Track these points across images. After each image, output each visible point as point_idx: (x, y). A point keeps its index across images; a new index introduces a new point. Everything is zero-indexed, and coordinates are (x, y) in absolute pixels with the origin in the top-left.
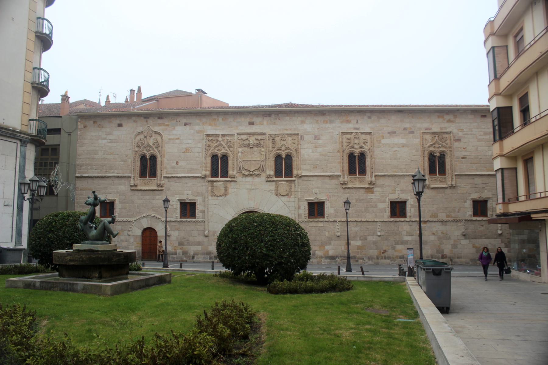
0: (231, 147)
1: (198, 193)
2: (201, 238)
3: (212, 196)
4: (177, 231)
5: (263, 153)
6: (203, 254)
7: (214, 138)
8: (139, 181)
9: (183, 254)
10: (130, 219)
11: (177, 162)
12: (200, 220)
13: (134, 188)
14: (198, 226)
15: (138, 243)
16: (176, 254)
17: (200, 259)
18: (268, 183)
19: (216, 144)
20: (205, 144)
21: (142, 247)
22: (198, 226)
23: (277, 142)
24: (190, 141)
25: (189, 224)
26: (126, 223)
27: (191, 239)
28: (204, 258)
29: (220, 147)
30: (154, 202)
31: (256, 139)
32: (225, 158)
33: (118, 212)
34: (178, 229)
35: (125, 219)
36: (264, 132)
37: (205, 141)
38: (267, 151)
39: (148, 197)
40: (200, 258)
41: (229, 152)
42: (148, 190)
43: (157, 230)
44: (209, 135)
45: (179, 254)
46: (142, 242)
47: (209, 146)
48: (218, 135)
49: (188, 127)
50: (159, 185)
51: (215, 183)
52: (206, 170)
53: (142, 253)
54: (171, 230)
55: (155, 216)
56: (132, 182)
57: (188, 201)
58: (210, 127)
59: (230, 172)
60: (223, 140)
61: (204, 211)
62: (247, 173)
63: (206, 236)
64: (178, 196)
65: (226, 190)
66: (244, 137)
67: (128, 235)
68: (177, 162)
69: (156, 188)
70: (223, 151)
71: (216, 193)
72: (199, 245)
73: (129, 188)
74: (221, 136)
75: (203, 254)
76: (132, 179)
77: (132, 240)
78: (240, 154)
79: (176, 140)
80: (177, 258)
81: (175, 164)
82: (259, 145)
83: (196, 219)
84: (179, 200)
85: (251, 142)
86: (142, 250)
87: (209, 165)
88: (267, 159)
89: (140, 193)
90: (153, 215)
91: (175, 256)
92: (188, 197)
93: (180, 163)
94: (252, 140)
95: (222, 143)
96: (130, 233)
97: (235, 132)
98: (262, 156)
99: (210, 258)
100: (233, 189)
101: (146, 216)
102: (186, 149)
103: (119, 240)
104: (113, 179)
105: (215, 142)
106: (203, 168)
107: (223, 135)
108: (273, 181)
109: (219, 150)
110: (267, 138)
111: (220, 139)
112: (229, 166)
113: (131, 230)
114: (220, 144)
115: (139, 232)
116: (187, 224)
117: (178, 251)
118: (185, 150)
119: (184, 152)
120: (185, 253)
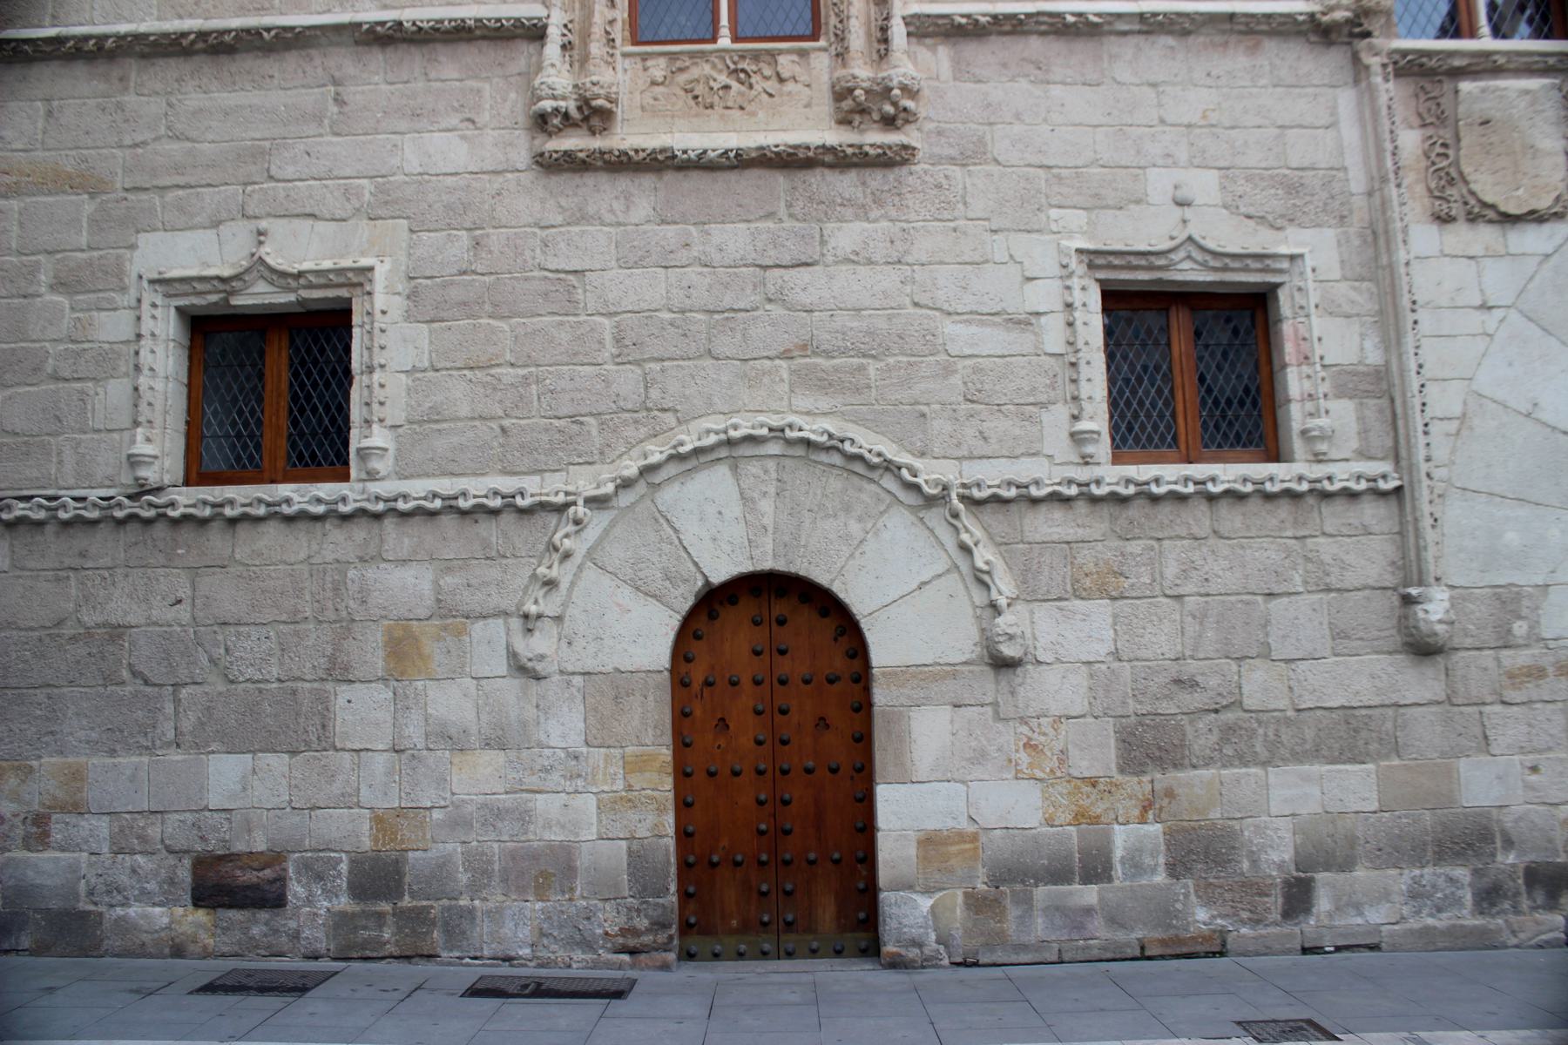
1: (1293, 188)
2: (1370, 677)
3: (1444, 219)
4: (1100, 610)
6: (1403, 850)
8: (620, 76)
9: (1174, 870)
10: (534, 488)
12: (1342, 474)
13: (575, 146)
14: (1326, 548)
15: (633, 766)
16: (1095, 868)
17: (1376, 916)
21: (683, 805)
22: (1326, 548)
25: (1232, 519)
26: (488, 530)
27: (1260, 686)
28: (1416, 894)
30: (807, 286)
33: (395, 413)
34: (1105, 585)
35: (477, 487)
39: (734, 239)
40: (1367, 901)
42: (740, 162)
43: (858, 596)
45: (1135, 865)
46: (681, 744)
50: (851, 105)
51: (1466, 86)
53: (684, 866)
54: (1030, 595)
55: (833, 446)
56: (558, 79)
57: (1189, 272)
63: (1423, 649)
64: (1076, 218)
67: (523, 670)
69: (822, 133)
72: (1356, 757)
73: (520, 147)
75: (1403, 850)
76: (552, 50)
77: (565, 726)
80: (1113, 921)
83: (1299, 467)
84: (1093, 258)
86: (684, 835)
89: (642, 197)
90: (813, 429)
91: (1090, 894)
92: (1190, 221)
96: (541, 643)
99: (1489, 896)
101: (732, 447)
103: (414, 733)
104: (343, 61)
113: (550, 606)
115: (646, 637)
116: (1198, 518)
117: (1121, 838)
120: (1200, 852)
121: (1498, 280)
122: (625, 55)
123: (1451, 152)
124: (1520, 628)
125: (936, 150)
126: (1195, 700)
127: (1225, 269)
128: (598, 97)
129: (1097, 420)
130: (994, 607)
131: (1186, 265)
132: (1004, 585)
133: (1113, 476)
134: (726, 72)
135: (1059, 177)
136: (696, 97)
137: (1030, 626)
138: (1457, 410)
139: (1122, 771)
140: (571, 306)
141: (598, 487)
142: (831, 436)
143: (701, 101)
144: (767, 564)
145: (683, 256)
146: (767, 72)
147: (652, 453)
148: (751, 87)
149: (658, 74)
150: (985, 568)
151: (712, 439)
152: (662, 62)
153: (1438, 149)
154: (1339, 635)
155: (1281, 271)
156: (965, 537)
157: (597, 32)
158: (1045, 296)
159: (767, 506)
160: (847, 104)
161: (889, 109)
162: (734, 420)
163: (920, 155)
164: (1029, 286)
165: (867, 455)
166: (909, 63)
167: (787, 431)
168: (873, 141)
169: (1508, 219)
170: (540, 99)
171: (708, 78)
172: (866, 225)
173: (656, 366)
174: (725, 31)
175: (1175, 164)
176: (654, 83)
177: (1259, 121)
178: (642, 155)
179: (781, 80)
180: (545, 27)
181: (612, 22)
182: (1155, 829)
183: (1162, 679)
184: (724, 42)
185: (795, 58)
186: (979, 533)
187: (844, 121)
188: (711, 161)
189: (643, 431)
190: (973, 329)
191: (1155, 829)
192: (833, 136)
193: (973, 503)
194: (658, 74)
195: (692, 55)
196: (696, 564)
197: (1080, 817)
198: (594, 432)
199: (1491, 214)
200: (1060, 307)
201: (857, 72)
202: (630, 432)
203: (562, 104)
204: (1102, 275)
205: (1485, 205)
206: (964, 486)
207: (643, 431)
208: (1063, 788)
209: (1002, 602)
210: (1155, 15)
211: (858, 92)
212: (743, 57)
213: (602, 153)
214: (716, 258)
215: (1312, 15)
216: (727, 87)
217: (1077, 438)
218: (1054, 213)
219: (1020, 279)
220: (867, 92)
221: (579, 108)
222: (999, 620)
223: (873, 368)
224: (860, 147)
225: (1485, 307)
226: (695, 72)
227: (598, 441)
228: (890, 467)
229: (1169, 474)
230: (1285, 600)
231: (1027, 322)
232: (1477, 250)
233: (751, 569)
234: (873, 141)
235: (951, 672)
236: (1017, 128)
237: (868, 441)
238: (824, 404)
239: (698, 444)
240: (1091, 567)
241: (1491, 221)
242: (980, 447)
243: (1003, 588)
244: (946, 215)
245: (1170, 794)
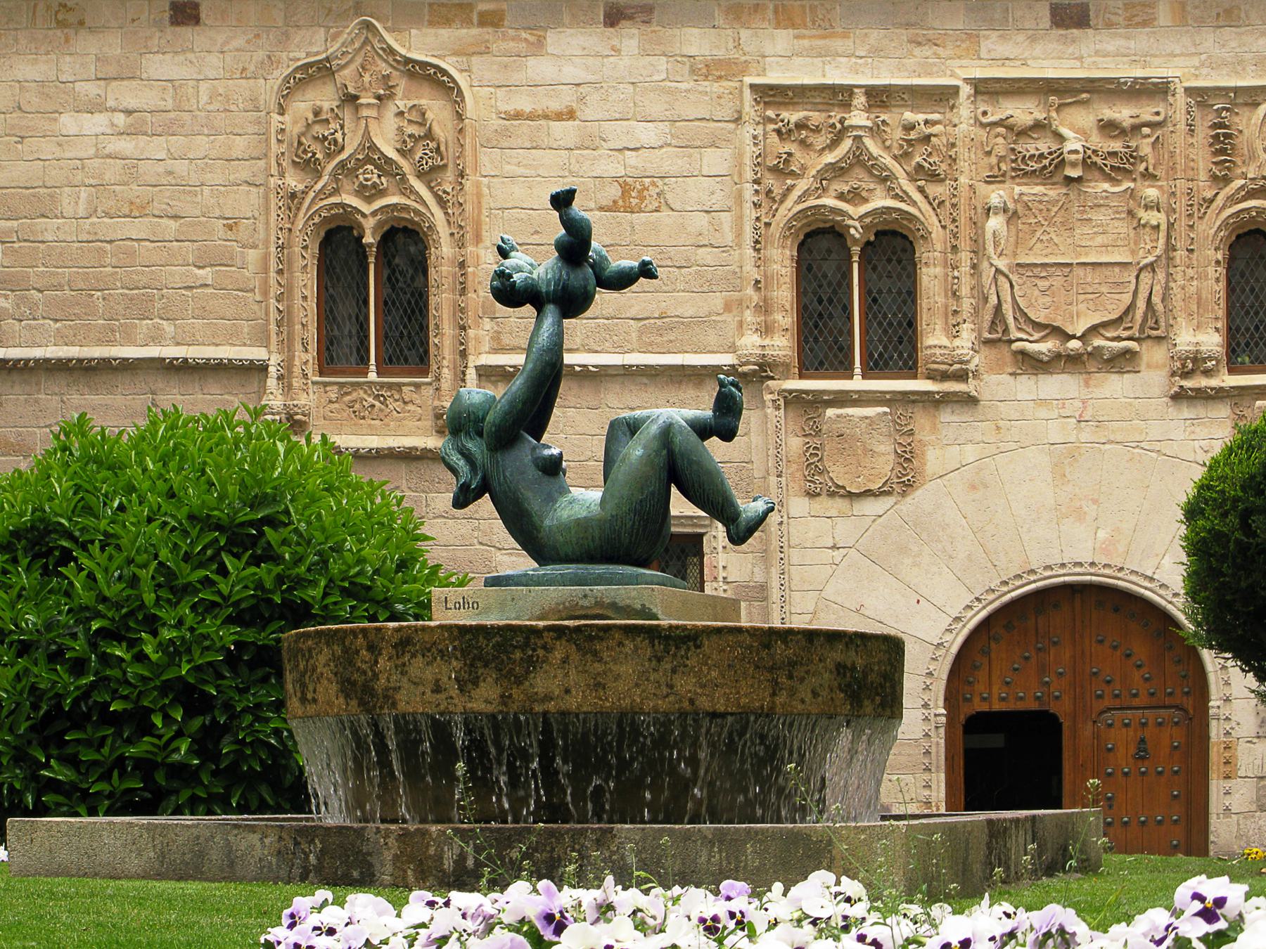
0: (934, 177)
3: (812, 495)
5: (1154, 217)
7: (816, 117)
18: (1187, 412)
19: (830, 158)
20: (750, 150)
23: (1241, 142)
24: (647, 134)
29: (859, 180)
32: (893, 245)
36: (1156, 71)
37: (748, 131)
38: (1181, 204)
41: (921, 209)
44: (772, 87)
47: (782, 170)
48: (839, 96)
49: (629, 38)
52: (766, 329)
58: (782, 40)
59: (934, 339)
60: (877, 131)
61: (763, 588)
62: (1046, 347)
65: (906, 456)
66: (1023, 111)
70: (880, 201)
71: (839, 473)
74: (860, 100)
78: (995, 223)
79: (556, 126)
82: (1121, 167)
85: (1073, 143)
87: (785, 294)
88: (1180, 255)
94: (1077, 131)
95: (872, 145)
97: (957, 71)
98: (1147, 235)
100: (947, 445)
102: (626, 189)
105: (820, 141)
106: (749, 316)
107: (879, 97)
108: (1219, 395)
109: (854, 196)
110: (1180, 117)
111: (858, 118)
112: (924, 303)
114: (859, 159)
118: (614, 191)
121: (844, 530)
138: (811, 610)
143: (359, 414)
146: (397, 397)
149: (333, 396)
152: (335, 388)
153: (811, 451)
155: (705, 526)
157: (297, 371)
169: (851, 495)
171: (362, 399)
174: (373, 368)
176: (331, 402)
179: (405, 403)
184: (372, 376)
194: (333, 396)
195: (352, 384)
203: (277, 417)
205: (838, 486)
212: (382, 387)
225: (834, 547)
226: (355, 395)
232: (833, 513)
241: (842, 496)
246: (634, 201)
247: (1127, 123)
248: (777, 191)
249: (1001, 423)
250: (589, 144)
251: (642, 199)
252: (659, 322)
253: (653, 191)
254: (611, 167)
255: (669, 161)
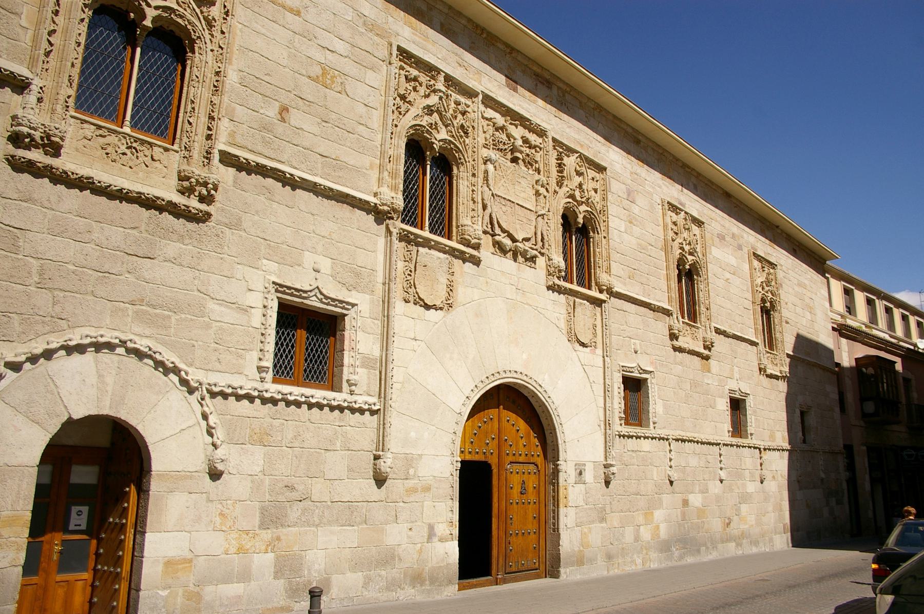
4: (259, 452)
11: (284, 110)
12: (361, 400)
24: (340, 46)
27: (318, 490)
31: (526, 141)
34: (262, 439)
36: (544, 125)
54: (231, 442)
57: (314, 302)
64: (273, 266)
68: (284, 110)
81: (272, 112)
84: (279, 287)
90: (142, 344)
92: (317, 279)
93: (295, 117)
102: (324, 73)
118: (317, 71)
119: (315, 80)
122: (72, 117)
123: (413, 274)
124: (412, 471)
125: (220, 218)
126: (295, 495)
127: (328, 304)
128: (56, 136)
129: (269, 363)
130: (215, 446)
131: (314, 298)
132: (220, 434)
133: (274, 389)
134: (125, 146)
135: (269, 245)
136: (107, 154)
137: (229, 456)
139: (260, 528)
140: (15, 248)
141: (16, 356)
142: (150, 349)
144: (105, 411)
145: (86, 237)
147: (53, 342)
148: (137, 157)
150: (214, 425)
151: (87, 341)
154: (350, 470)
155: (348, 309)
156: (206, 409)
158: (255, 299)
159: (110, 380)
160: (186, 184)
161: (204, 192)
162: (102, 333)
163: (212, 218)
164: (249, 293)
165: (167, 362)
166: (225, 175)
167: (129, 343)
168: (192, 207)
169: (427, 307)
170: (20, 125)
172: (181, 245)
173: (61, 294)
175: (316, 253)
177: (350, 242)
178: (75, 176)
179: (153, 160)
180: (29, 84)
181: (69, 97)
182: (271, 556)
183: (281, 485)
184: (127, 129)
185: (162, 150)
186: (212, 409)
187: (182, 192)
188: (112, 191)
189: (47, 328)
190: (223, 309)
191: (271, 556)
192: (177, 198)
193: (213, 395)
194: (89, 134)
195: (110, 130)
196: (66, 407)
197: (241, 550)
198: (16, 324)
199: (422, 303)
200: (261, 306)
201: (194, 170)
202: (39, 328)
204: (280, 295)
205: (420, 298)
206: (209, 384)
207: (47, 328)
208: (234, 535)
209: (219, 443)
210: (320, 185)
211: (193, 180)
212: (136, 141)
213: (52, 168)
214: (105, 243)
215: (376, 204)
216: (124, 154)
217: (260, 369)
218: (265, 261)
219: (246, 289)
220: (197, 180)
221: (42, 138)
222: (216, 452)
223: (174, 318)
224: (188, 207)
227: (18, 329)
228: (176, 371)
229: (295, 392)
230: (332, 453)
231: (246, 310)
233: (96, 413)
234: (192, 207)
235: (189, 476)
236: (256, 218)
237: (169, 357)
238: (148, 332)
239: (81, 342)
240: (257, 431)
242: (218, 366)
243: (220, 437)
244: (219, 250)
245: (278, 539)
246: (329, 82)
247: (533, 143)
248: (402, 110)
249: (489, 280)
250: (309, 37)
251: (333, 82)
252: (335, 162)
253: (339, 80)
254: (319, 56)
255: (348, 67)
